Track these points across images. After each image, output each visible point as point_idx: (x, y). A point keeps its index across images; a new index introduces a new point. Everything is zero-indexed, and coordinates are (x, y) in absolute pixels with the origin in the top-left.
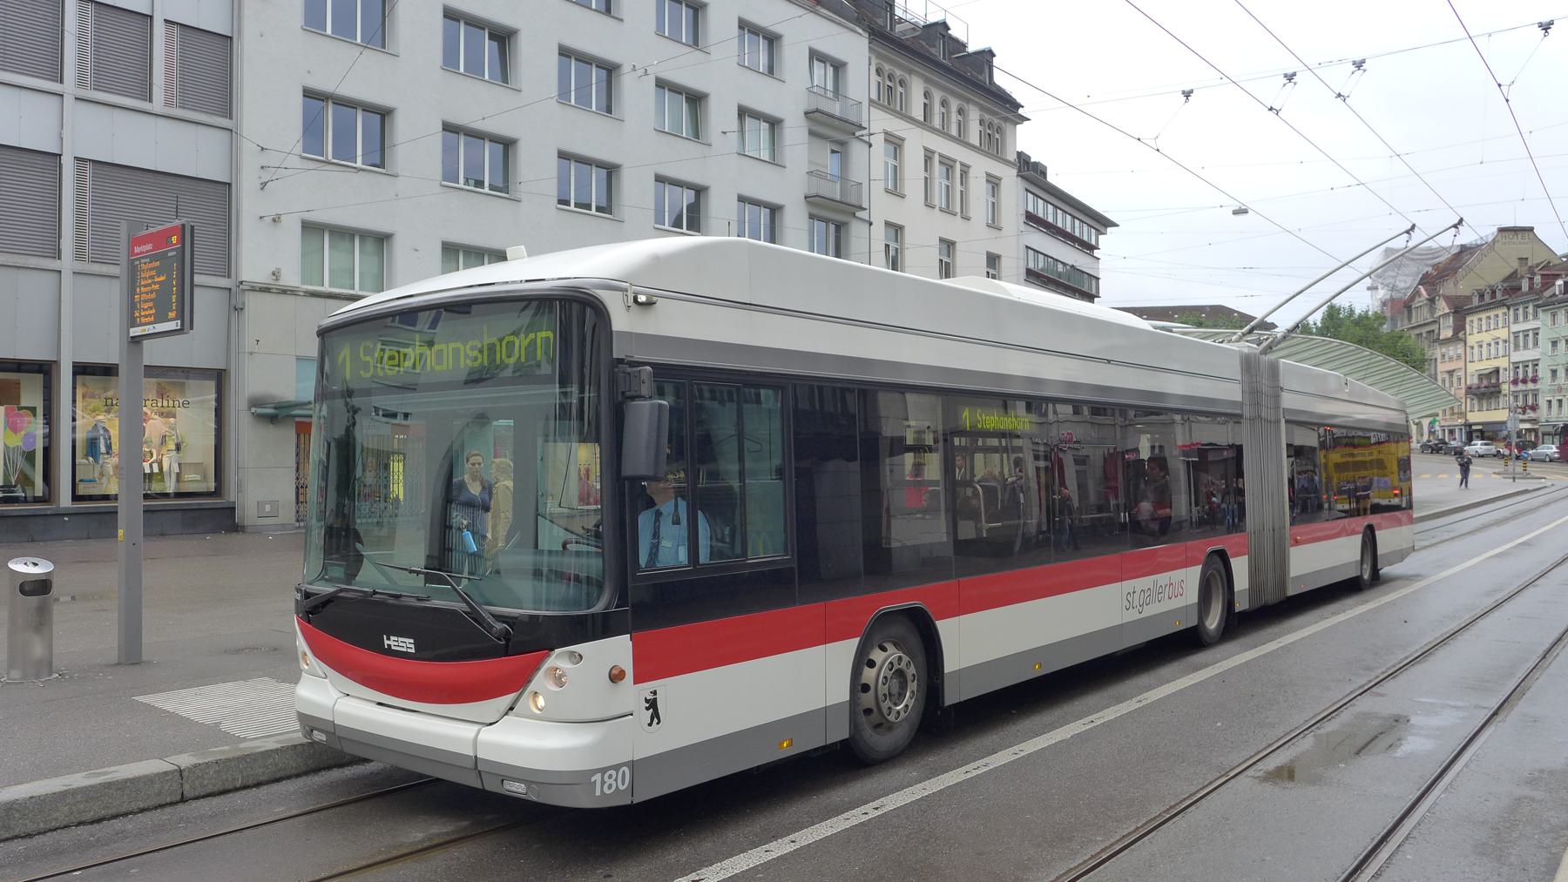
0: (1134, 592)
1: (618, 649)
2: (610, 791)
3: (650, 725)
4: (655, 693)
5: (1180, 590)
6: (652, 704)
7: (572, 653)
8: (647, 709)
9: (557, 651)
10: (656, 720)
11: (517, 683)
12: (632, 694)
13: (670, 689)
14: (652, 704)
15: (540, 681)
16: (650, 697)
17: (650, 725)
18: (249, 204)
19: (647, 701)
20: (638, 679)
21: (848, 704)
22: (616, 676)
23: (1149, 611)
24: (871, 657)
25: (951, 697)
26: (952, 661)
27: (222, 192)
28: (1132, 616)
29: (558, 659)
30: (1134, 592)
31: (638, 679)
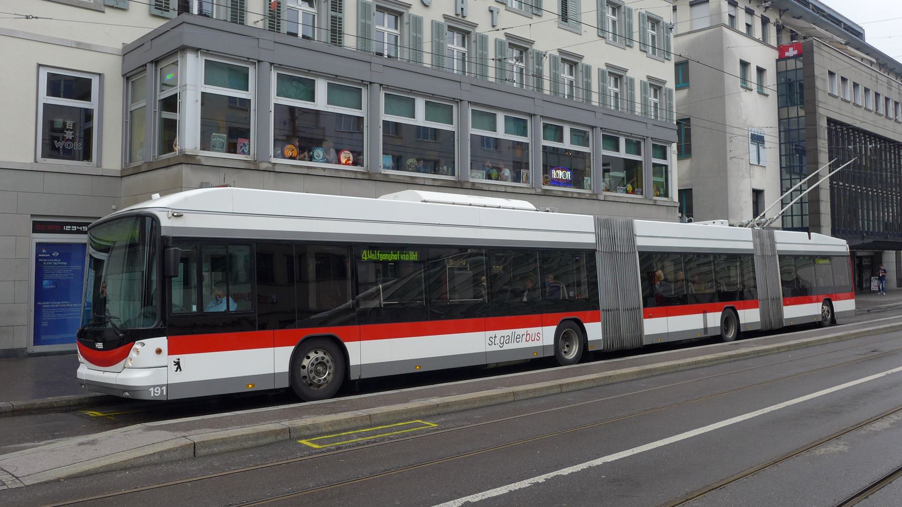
0: (495, 337)
1: (162, 342)
2: (155, 394)
3: (176, 371)
4: (179, 359)
5: (536, 337)
6: (178, 364)
7: (142, 343)
8: (175, 365)
9: (136, 342)
10: (179, 370)
11: (125, 355)
12: (168, 359)
13: (186, 359)
14: (178, 364)
15: (132, 354)
16: (177, 361)
17: (176, 371)
19: (174, 362)
20: (170, 353)
21: (288, 373)
22: (159, 351)
23: (506, 347)
24: (309, 355)
25: (354, 376)
26: (354, 361)
28: (496, 348)
29: (137, 345)
30: (495, 337)
31: (170, 353)
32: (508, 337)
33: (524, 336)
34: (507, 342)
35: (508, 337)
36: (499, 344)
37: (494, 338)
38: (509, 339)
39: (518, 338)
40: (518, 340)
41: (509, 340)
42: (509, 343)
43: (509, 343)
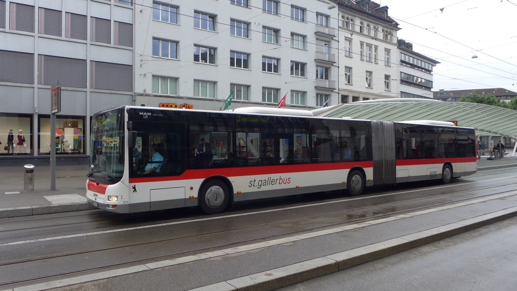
0: (255, 181)
5: (287, 181)
18: (137, 71)
23: (263, 188)
27: (129, 68)
30: (255, 181)
32: (265, 181)
33: (278, 181)
34: (264, 184)
35: (265, 181)
36: (258, 186)
37: (253, 182)
38: (266, 182)
39: (273, 182)
40: (273, 183)
41: (265, 183)
42: (265, 185)
43: (265, 185)
